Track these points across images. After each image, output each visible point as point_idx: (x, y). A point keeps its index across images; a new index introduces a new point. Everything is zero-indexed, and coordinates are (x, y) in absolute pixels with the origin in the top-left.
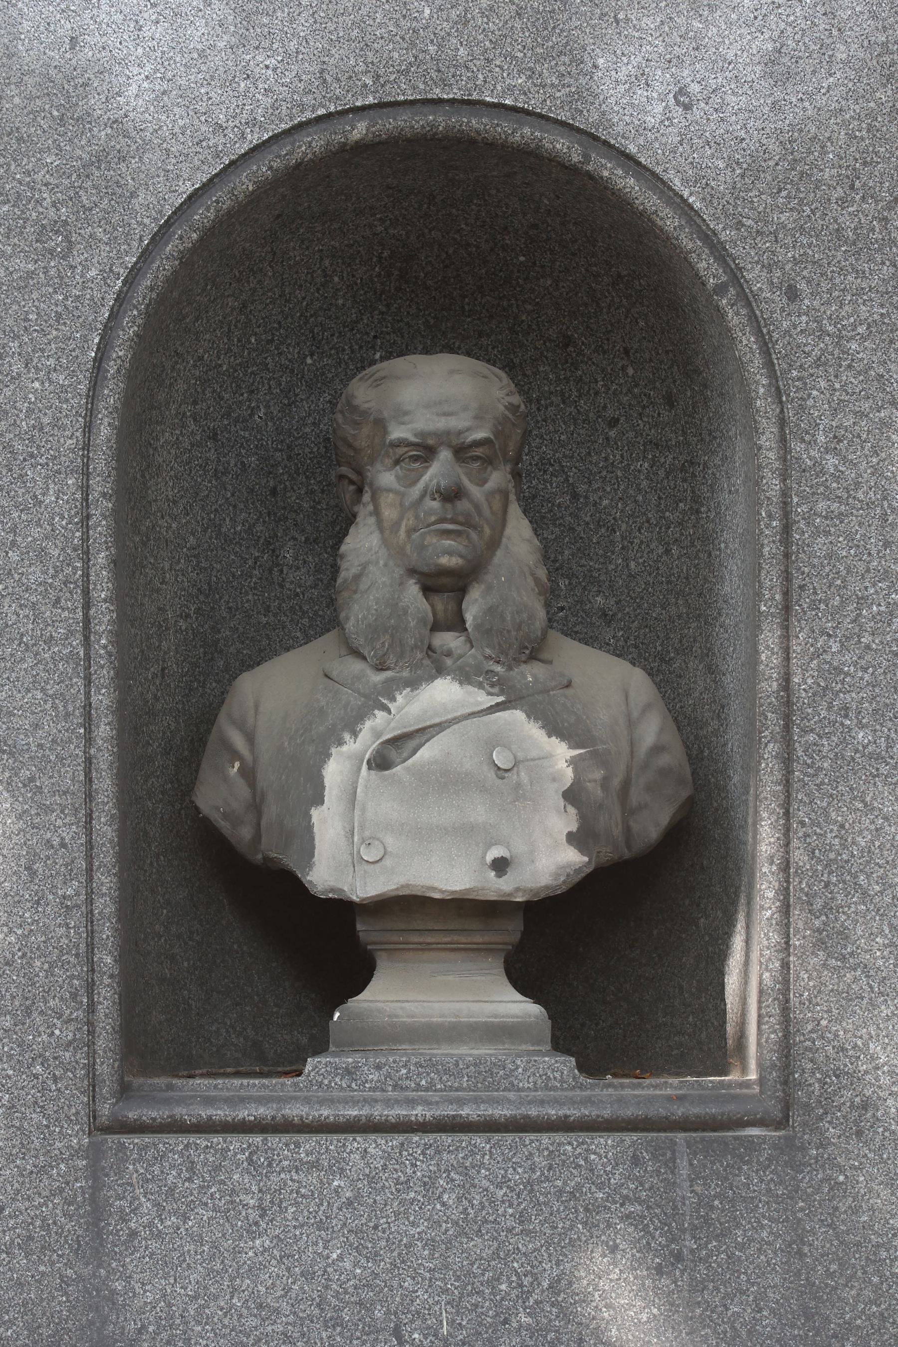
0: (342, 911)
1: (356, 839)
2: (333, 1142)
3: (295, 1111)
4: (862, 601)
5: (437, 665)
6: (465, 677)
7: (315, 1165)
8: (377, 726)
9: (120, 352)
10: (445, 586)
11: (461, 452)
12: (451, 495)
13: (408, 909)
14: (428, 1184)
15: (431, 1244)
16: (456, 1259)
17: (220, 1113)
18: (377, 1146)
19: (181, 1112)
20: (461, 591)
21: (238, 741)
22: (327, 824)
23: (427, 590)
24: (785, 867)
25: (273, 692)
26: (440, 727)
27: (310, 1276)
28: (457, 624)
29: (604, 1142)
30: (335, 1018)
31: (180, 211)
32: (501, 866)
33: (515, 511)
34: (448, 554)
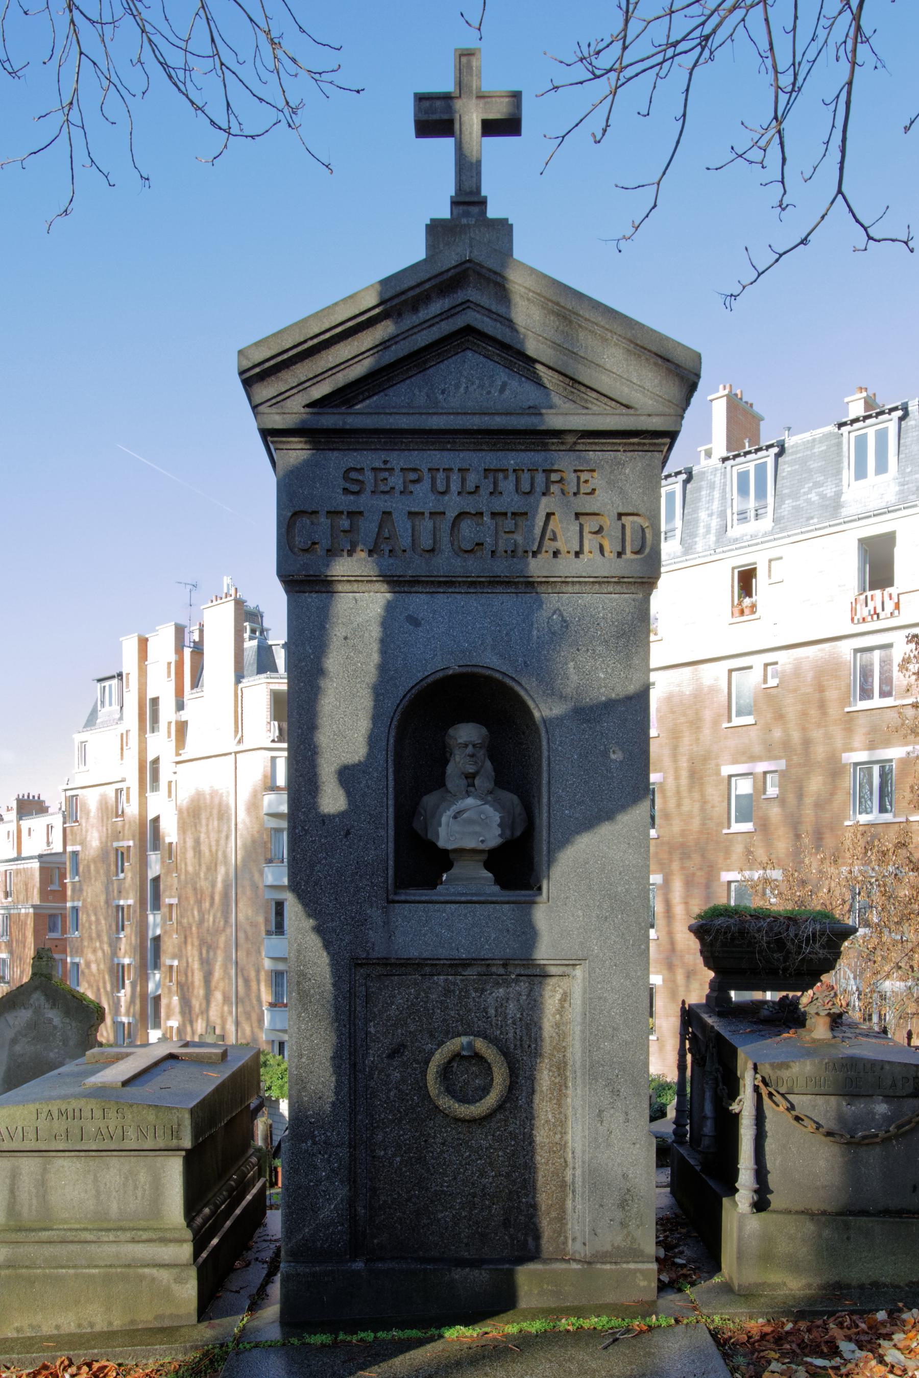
0: (446, 852)
1: (450, 832)
2: (443, 905)
3: (435, 898)
4: (567, 780)
5: (468, 794)
6: (476, 797)
7: (439, 911)
8: (455, 808)
9: (395, 723)
10: (470, 777)
11: (474, 746)
12: (472, 756)
13: (461, 851)
14: (465, 915)
15: (466, 929)
16: (471, 933)
17: (417, 898)
18: (453, 906)
19: (408, 898)
20: (474, 778)
21: (423, 812)
22: (442, 831)
23: (466, 778)
24: (549, 842)
25: (429, 800)
26: (469, 809)
27: (437, 936)
28: (474, 785)
29: (506, 906)
30: (444, 878)
31: (409, 691)
32: (482, 841)
33: (487, 759)
34: (471, 769)
